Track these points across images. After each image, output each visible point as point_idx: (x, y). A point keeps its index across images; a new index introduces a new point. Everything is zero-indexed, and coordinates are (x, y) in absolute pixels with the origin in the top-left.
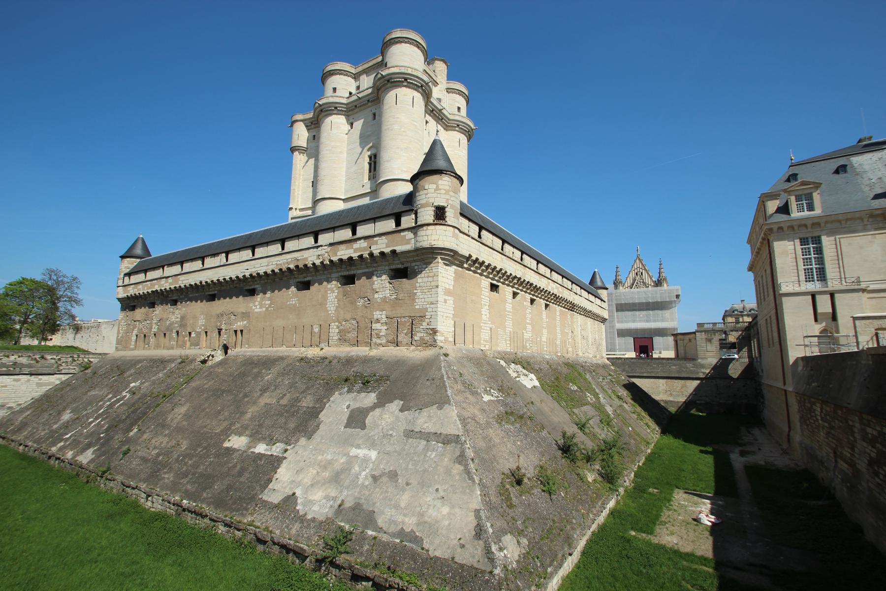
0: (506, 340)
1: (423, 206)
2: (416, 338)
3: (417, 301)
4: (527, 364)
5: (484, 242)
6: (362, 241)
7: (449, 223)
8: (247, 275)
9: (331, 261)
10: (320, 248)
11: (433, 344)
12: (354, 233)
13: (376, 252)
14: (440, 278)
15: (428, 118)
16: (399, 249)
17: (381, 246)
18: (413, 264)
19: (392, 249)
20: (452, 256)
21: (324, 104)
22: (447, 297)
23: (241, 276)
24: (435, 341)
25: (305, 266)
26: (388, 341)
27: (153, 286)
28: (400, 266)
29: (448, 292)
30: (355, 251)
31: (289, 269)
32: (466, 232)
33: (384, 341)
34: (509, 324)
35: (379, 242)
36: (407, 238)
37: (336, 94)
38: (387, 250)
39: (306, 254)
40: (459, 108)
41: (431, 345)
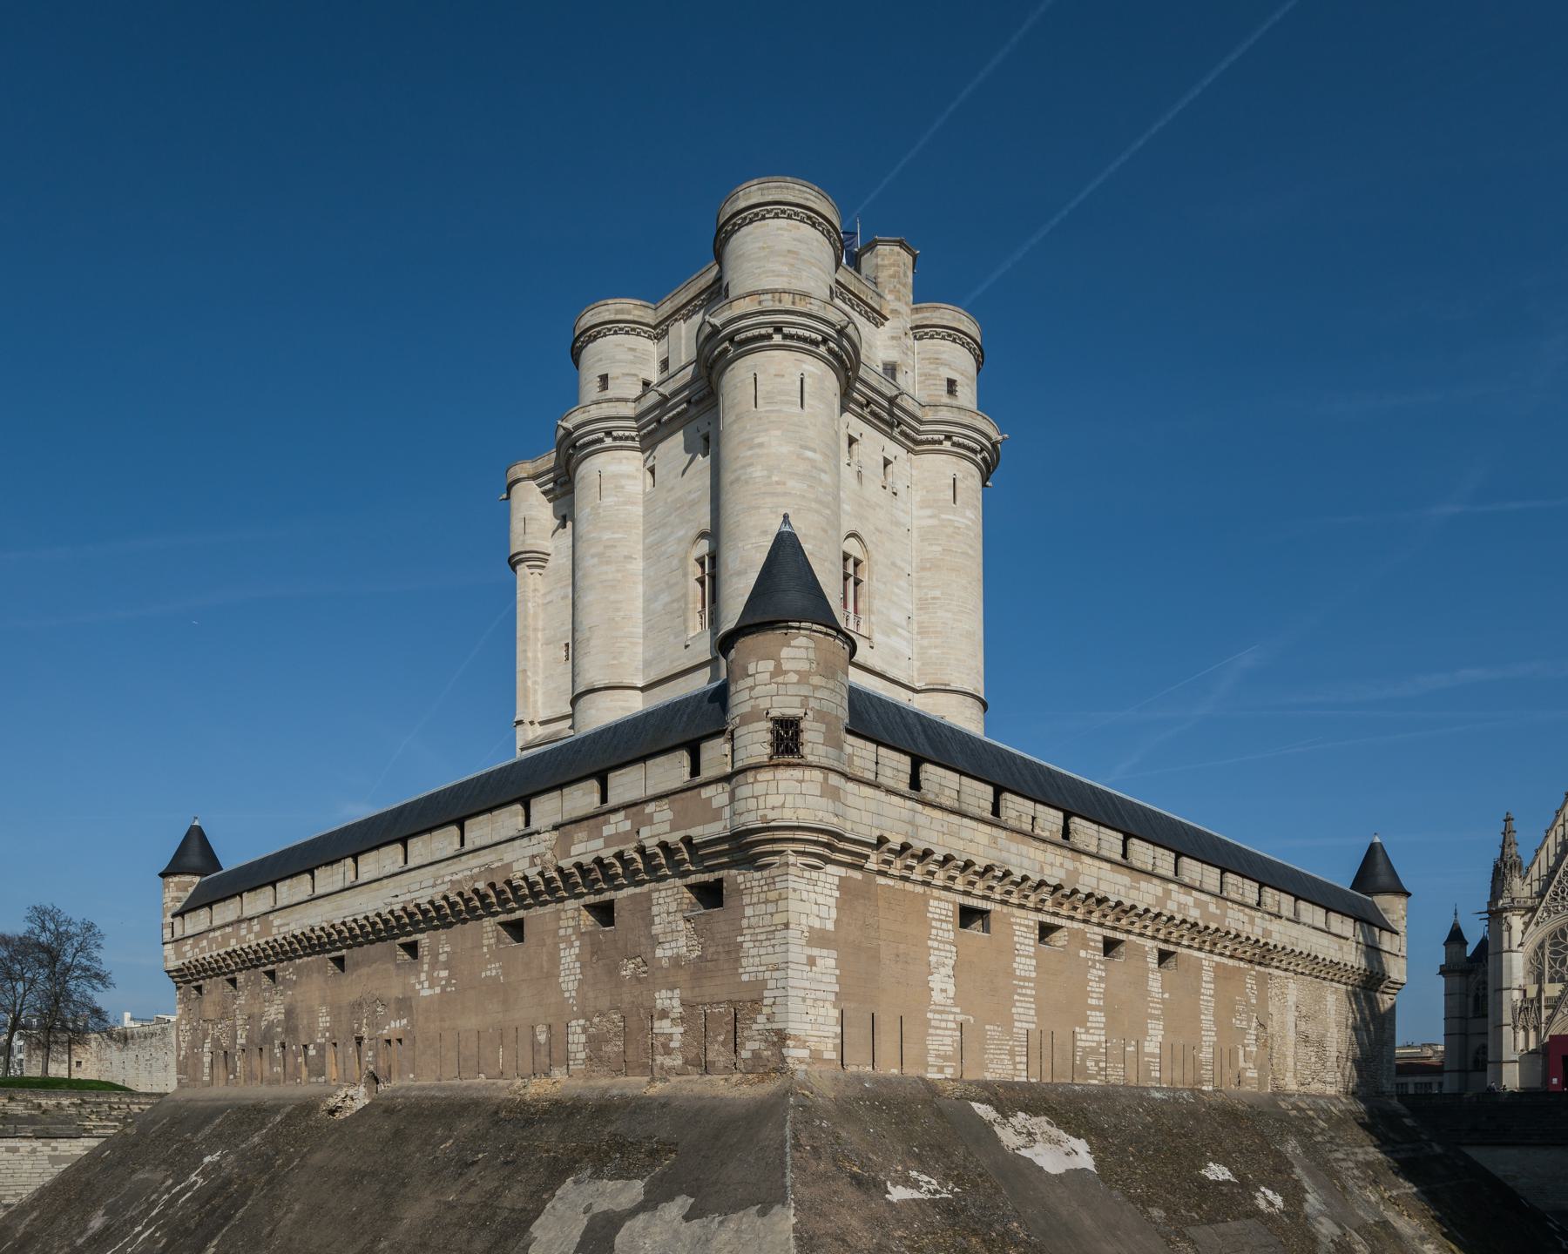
0: (1012, 1054)
2: (745, 1054)
3: (744, 962)
4: (1068, 1109)
5: (930, 797)
6: (621, 815)
11: (781, 1067)
14: (793, 905)
15: (856, 426)
16: (700, 833)
17: (660, 827)
21: (577, 427)
22: (815, 952)
24: (783, 1059)
26: (686, 1062)
30: (609, 841)
33: (678, 1061)
35: (657, 817)
37: (610, 394)
40: (951, 384)
41: (775, 1070)
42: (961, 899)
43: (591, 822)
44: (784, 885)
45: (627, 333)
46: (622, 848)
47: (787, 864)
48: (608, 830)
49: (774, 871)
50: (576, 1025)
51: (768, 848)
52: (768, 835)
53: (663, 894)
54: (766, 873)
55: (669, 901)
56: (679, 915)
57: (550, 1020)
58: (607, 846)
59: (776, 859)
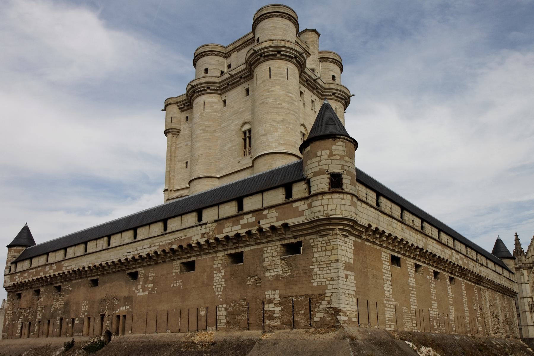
1: (316, 174)
6: (250, 215)
7: (346, 190)
8: (130, 257)
9: (217, 239)
10: (204, 227)
12: (240, 207)
13: (266, 227)
16: (291, 222)
17: (271, 220)
18: (308, 238)
19: (283, 222)
20: (352, 227)
23: (123, 259)
25: (189, 245)
27: (38, 273)
28: (292, 241)
29: (348, 267)
30: (243, 227)
31: (172, 249)
32: (364, 199)
34: (413, 300)
36: (300, 209)
38: (278, 224)
39: (190, 233)
42: (391, 253)
43: (234, 219)
44: (335, 243)
45: (216, 55)
46: (250, 229)
47: (337, 234)
48: (242, 222)
49: (329, 237)
50: (222, 308)
51: (328, 227)
52: (329, 222)
53: (270, 248)
54: (325, 238)
55: (272, 252)
56: (278, 258)
57: (207, 305)
58: (242, 228)
59: (331, 232)
